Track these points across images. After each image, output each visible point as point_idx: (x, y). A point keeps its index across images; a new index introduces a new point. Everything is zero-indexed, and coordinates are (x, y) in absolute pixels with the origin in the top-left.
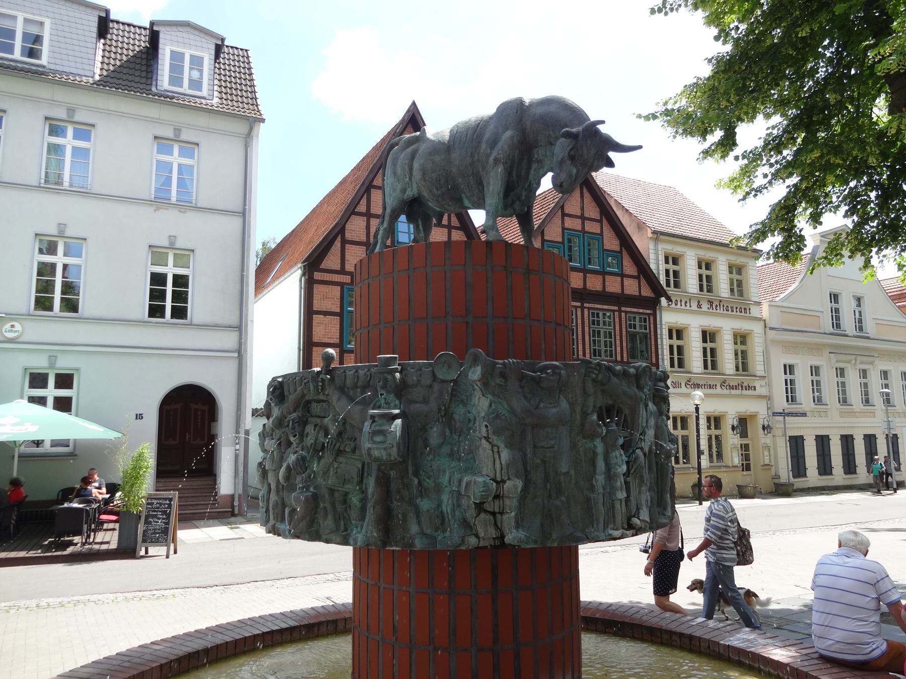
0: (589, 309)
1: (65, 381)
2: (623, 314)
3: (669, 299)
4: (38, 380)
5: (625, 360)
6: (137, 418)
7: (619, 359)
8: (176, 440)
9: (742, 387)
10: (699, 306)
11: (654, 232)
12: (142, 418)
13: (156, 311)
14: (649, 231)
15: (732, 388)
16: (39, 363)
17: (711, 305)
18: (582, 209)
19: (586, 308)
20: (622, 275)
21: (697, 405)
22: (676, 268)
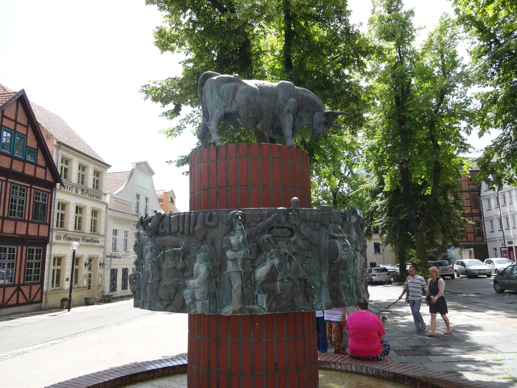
0: (11, 183)
2: (33, 190)
3: (62, 184)
5: (30, 220)
7: (26, 219)
9: (93, 240)
10: (77, 192)
11: (59, 143)
14: (55, 141)
15: (87, 241)
17: (83, 192)
18: (16, 116)
19: (9, 182)
20: (36, 165)
21: (74, 250)
22: (66, 166)
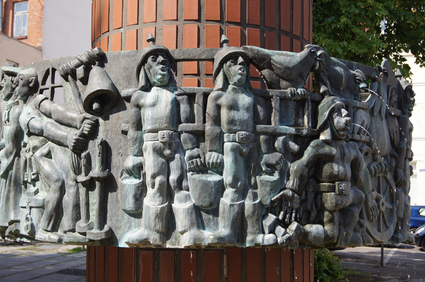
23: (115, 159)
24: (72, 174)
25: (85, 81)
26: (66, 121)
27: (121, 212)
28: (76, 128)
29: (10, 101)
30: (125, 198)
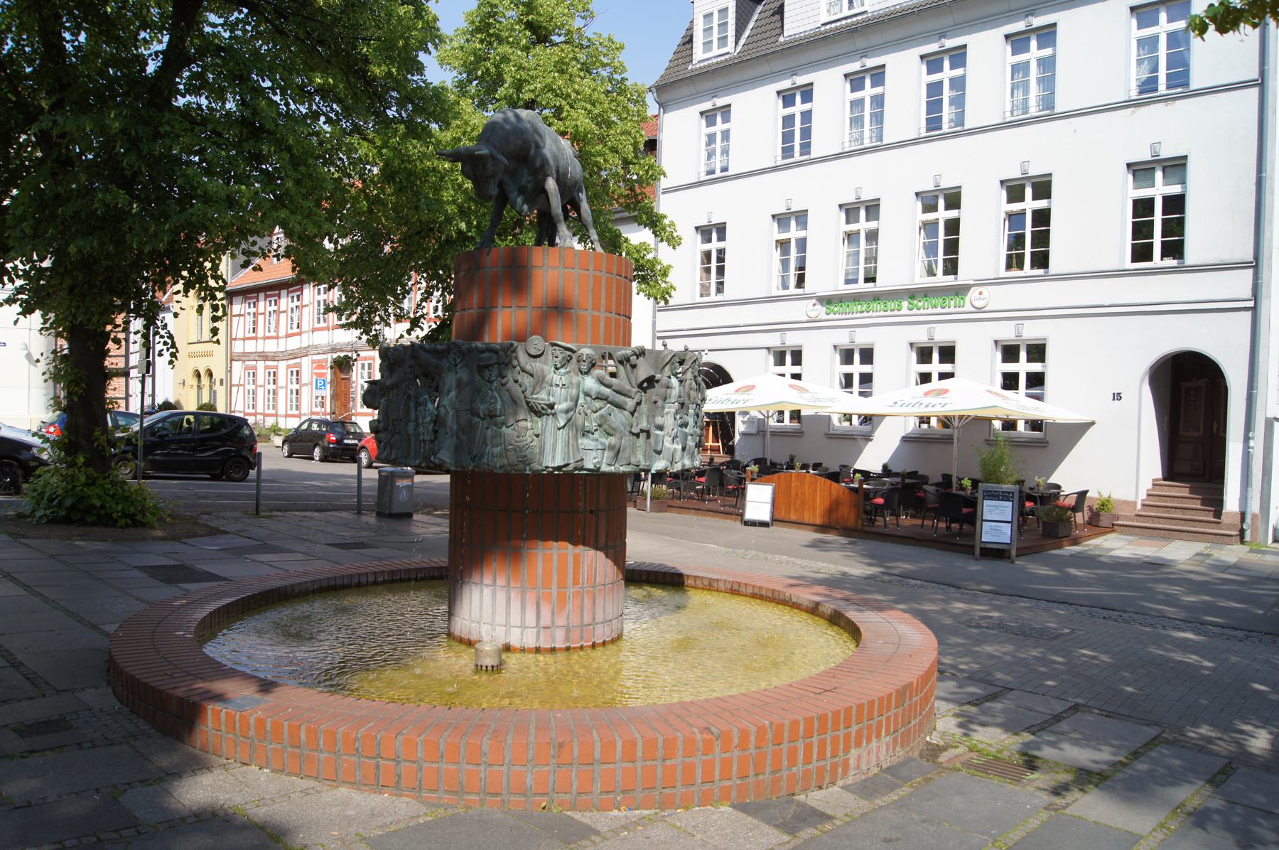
1: (1037, 352)
4: (1010, 353)
6: (1114, 399)
8: (1199, 431)
12: (1121, 398)
13: (1141, 253)
16: (1007, 332)
23: (651, 418)
24: (628, 428)
25: (634, 366)
26: (624, 392)
27: (652, 451)
28: (630, 397)
29: (562, 371)
30: (657, 443)
